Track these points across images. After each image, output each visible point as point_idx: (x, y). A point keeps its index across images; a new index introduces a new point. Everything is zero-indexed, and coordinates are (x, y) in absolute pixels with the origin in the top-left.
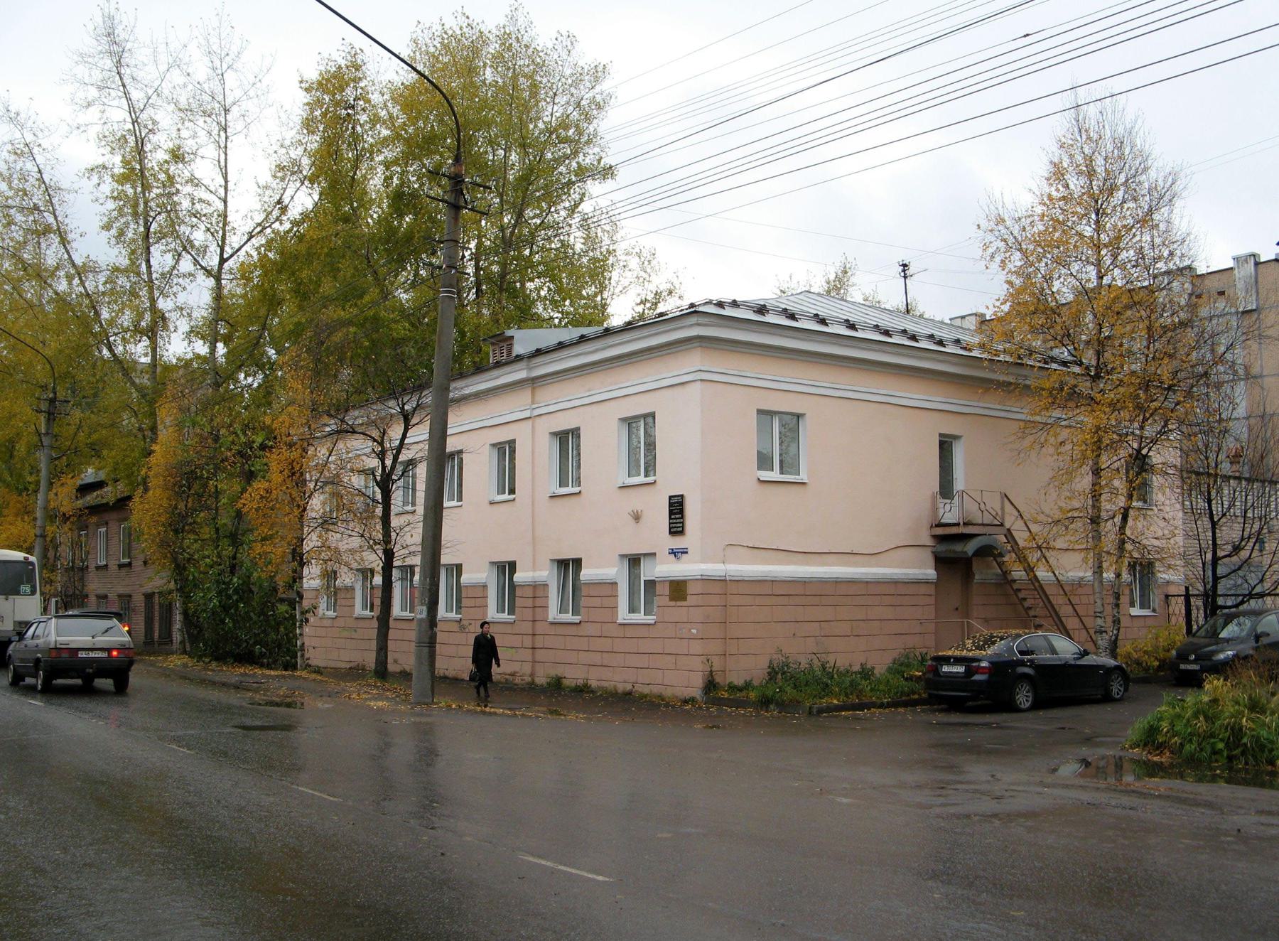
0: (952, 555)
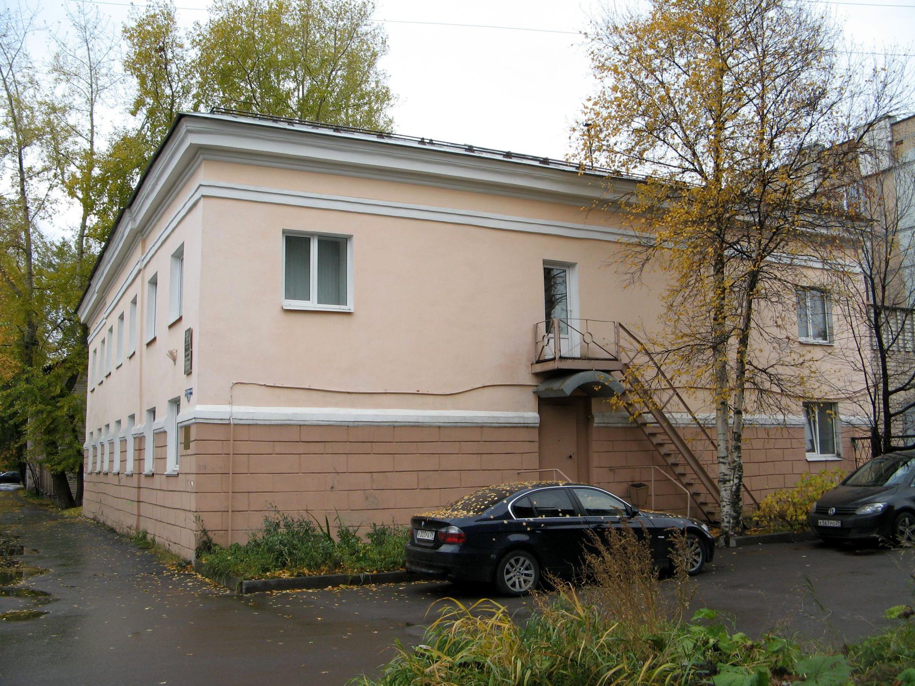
0: (552, 395)
